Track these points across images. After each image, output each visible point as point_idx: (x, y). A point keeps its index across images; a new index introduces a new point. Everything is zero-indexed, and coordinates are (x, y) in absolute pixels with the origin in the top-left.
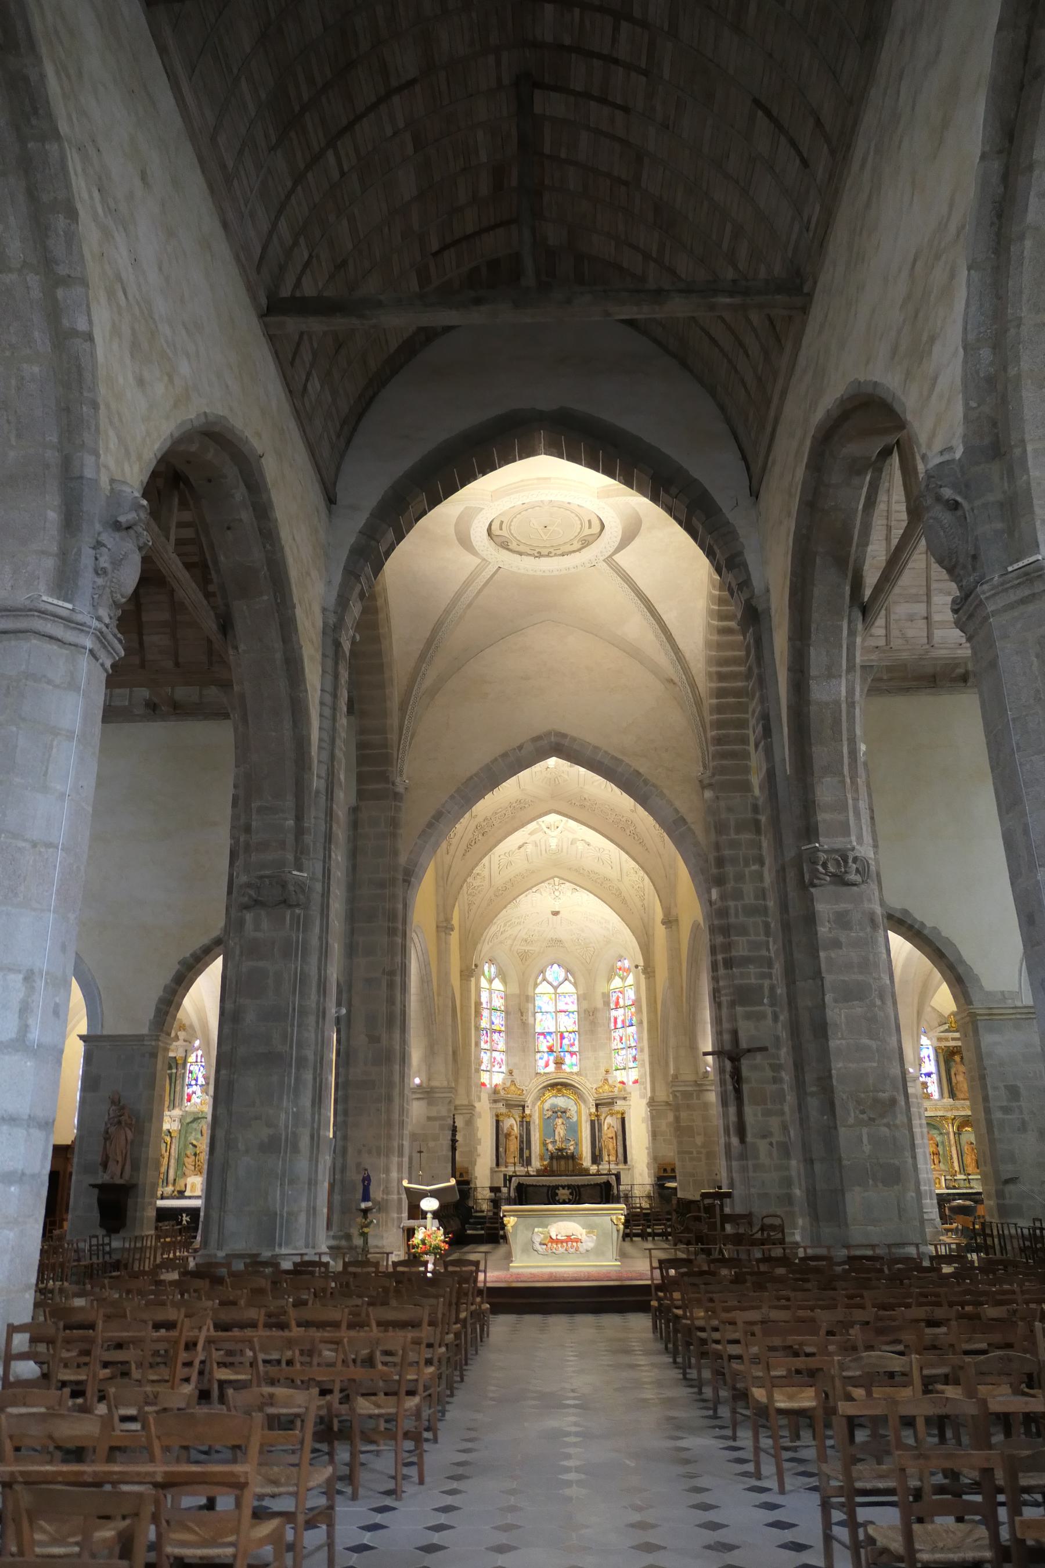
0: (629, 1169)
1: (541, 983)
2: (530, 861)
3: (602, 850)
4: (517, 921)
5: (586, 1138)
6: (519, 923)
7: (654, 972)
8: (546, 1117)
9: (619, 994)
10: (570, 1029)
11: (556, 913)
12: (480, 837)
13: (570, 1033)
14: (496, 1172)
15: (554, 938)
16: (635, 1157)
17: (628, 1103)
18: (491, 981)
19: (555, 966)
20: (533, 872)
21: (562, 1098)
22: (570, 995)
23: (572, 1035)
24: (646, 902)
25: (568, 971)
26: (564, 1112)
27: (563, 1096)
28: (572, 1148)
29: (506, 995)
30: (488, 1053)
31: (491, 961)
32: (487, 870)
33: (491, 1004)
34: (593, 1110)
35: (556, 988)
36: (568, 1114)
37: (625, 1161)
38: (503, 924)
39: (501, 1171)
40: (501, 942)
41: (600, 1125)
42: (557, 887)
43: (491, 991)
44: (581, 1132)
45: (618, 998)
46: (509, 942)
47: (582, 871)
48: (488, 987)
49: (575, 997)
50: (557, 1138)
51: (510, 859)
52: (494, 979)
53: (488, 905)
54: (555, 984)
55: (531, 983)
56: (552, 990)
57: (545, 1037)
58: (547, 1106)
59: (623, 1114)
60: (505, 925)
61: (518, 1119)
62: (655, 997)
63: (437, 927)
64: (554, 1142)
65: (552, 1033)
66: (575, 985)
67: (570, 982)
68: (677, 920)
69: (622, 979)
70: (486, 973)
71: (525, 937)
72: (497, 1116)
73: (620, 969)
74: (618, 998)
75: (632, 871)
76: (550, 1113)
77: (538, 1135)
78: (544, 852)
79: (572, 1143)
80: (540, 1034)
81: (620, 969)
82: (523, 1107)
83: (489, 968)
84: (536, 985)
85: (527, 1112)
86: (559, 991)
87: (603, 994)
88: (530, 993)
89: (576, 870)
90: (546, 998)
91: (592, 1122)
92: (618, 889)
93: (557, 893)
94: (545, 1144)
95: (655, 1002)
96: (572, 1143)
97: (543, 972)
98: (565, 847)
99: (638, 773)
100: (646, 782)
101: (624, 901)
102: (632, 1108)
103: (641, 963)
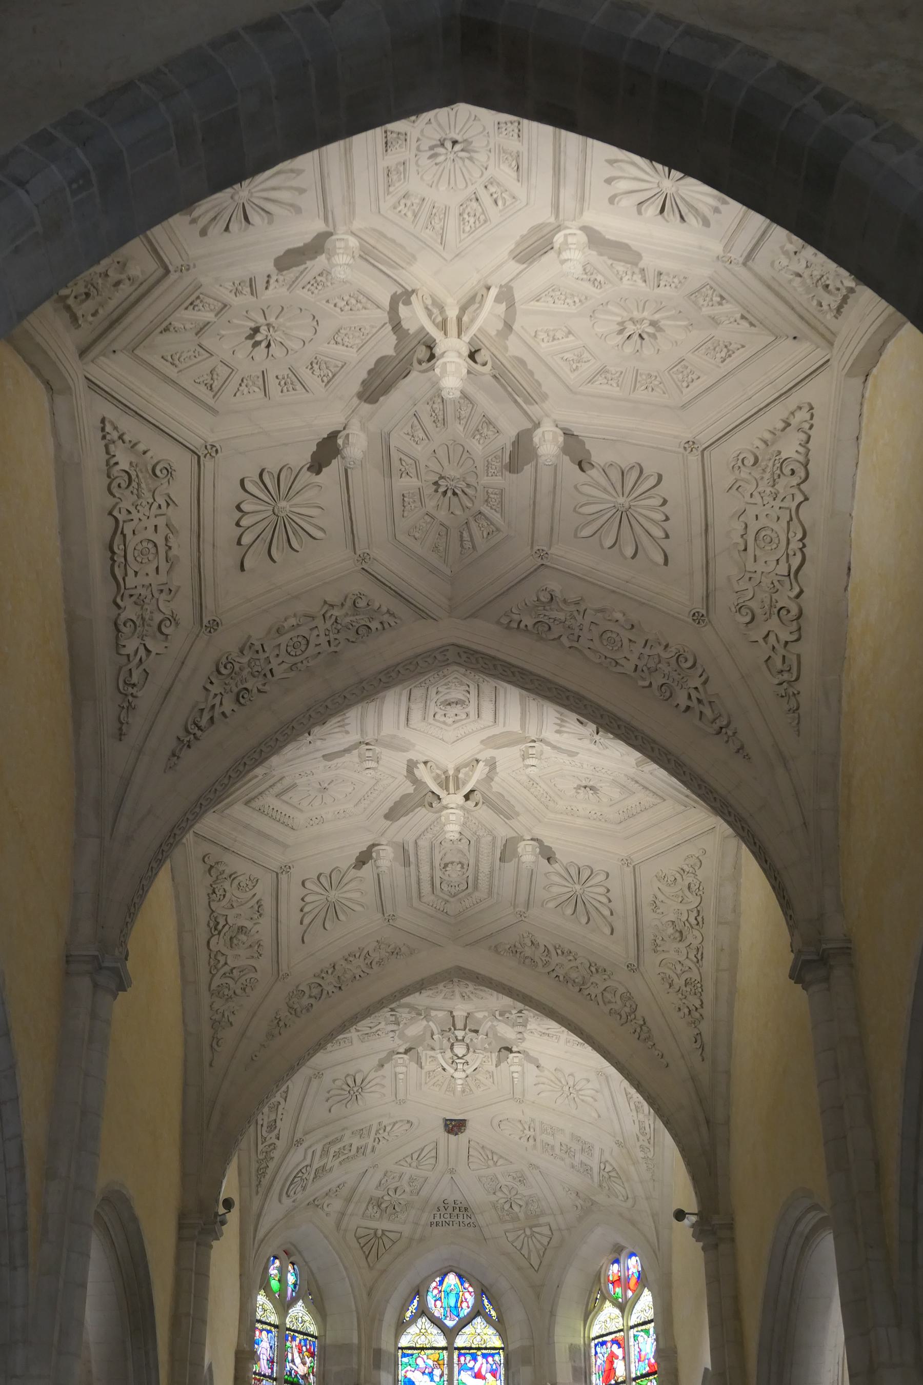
1: (414, 1319)
2: (389, 911)
3: (585, 874)
4: (356, 1142)
6: (362, 1151)
7: (731, 1227)
9: (615, 1347)
11: (455, 1126)
12: (228, 705)
15: (450, 1200)
18: (283, 1305)
19: (452, 1280)
20: (395, 952)
22: (488, 1352)
24: (705, 1027)
25: (483, 1291)
29: (323, 1348)
31: (289, 1255)
32: (181, 516)
33: (282, 1365)
35: (450, 1334)
38: (319, 1148)
40: (315, 1204)
42: (460, 1034)
43: (283, 1332)
45: (612, 1357)
46: (337, 1205)
47: (528, 952)
48: (273, 1319)
49: (500, 1358)
51: (333, 895)
52: (294, 1301)
53: (270, 1035)
54: (450, 1323)
55: (389, 1317)
56: (442, 1342)
60: (325, 1152)
62: (736, 1298)
63: (69, 959)
66: (500, 1326)
67: (488, 1319)
68: (846, 951)
69: (622, 1307)
70: (275, 1285)
71: (379, 1193)
73: (616, 1282)
74: (612, 1357)
75: (670, 930)
78: (426, 887)
81: (616, 1282)
83: (282, 1271)
84: (401, 1326)
86: (460, 1342)
87: (573, 1349)
88: (386, 1344)
89: (514, 951)
90: (425, 1360)
92: (627, 997)
93: (460, 1050)
95: (737, 1314)
97: (419, 1291)
98: (484, 868)
99: (797, 76)
100: (829, 101)
101: (643, 1033)
103: (691, 1204)
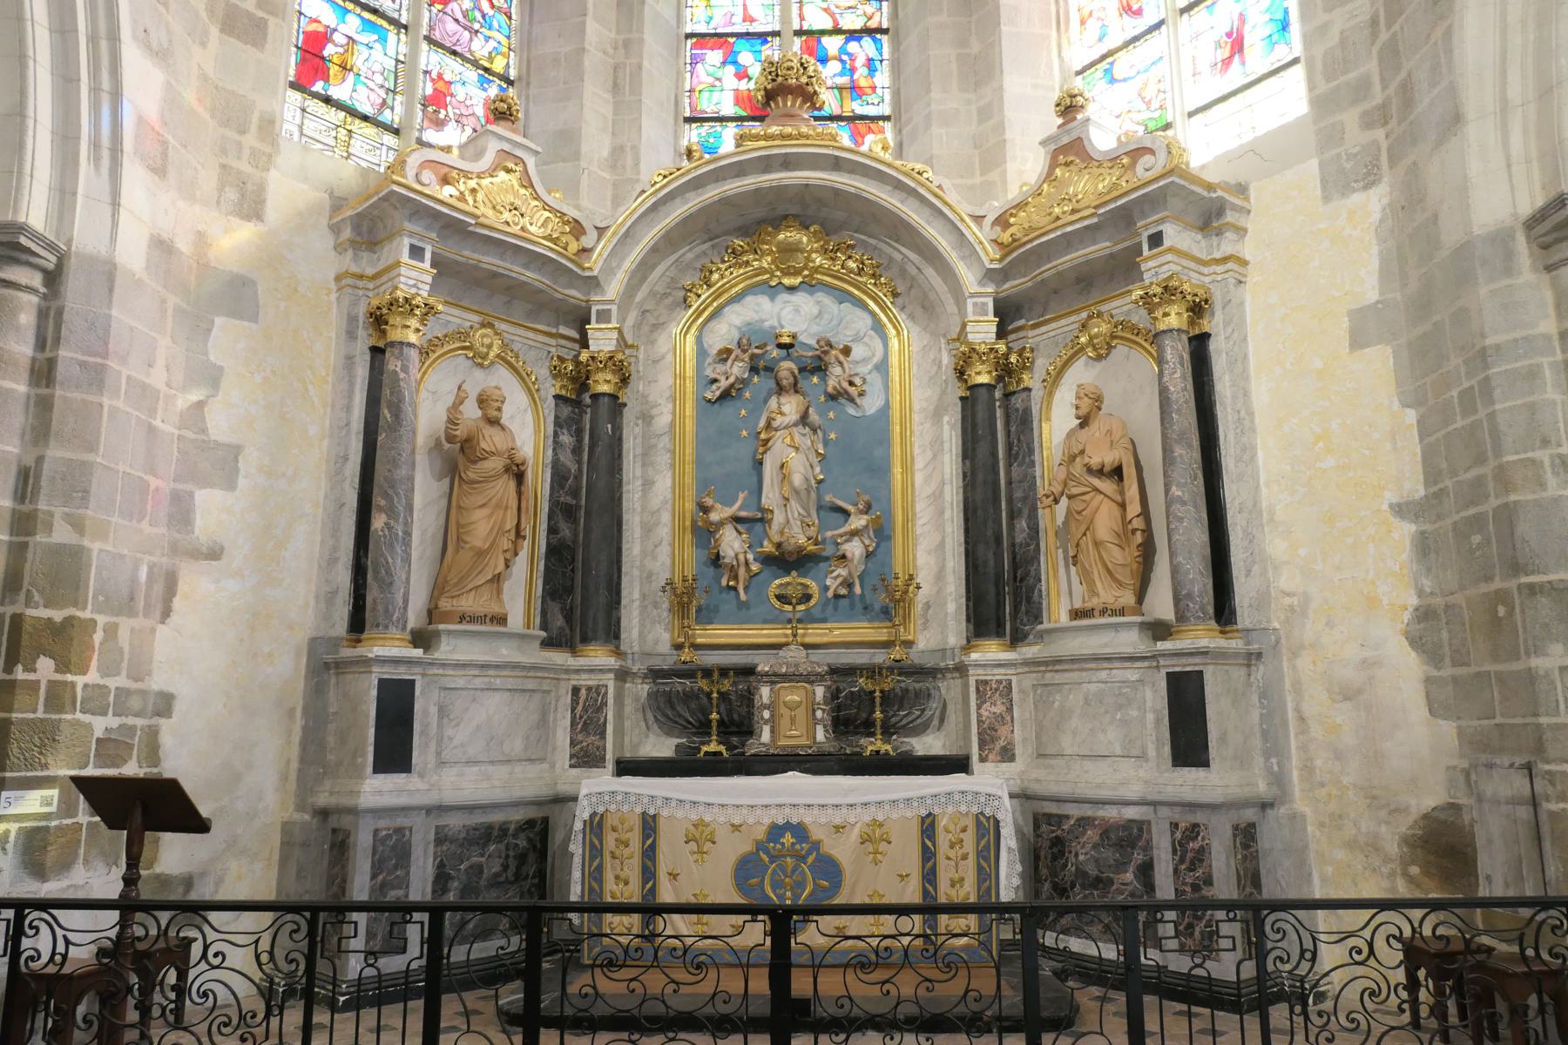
0: (1252, 658)
5: (937, 496)
8: (713, 393)
10: (852, 22)
13: (853, 35)
14: (340, 666)
16: (1286, 580)
17: (1227, 246)
21: (800, 298)
23: (864, 49)
26: (818, 367)
27: (810, 286)
28: (855, 549)
30: (396, 44)
34: (983, 331)
36: (836, 377)
37: (1223, 609)
39: (366, 662)
41: (1022, 425)
44: (908, 468)
50: (770, 497)
57: (730, 59)
58: (723, 333)
59: (1198, 309)
61: (551, 388)
64: (754, 522)
65: (763, 37)
72: (378, 320)
76: (738, 369)
77: (664, 484)
79: (858, 522)
80: (702, 39)
82: (581, 321)
85: (602, 340)
91: (973, 404)
94: (704, 533)
96: (858, 522)
102: (1253, 277)
